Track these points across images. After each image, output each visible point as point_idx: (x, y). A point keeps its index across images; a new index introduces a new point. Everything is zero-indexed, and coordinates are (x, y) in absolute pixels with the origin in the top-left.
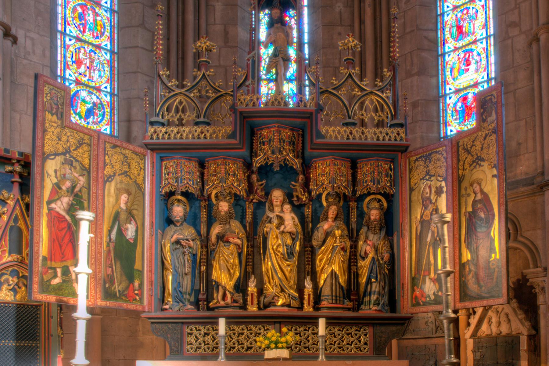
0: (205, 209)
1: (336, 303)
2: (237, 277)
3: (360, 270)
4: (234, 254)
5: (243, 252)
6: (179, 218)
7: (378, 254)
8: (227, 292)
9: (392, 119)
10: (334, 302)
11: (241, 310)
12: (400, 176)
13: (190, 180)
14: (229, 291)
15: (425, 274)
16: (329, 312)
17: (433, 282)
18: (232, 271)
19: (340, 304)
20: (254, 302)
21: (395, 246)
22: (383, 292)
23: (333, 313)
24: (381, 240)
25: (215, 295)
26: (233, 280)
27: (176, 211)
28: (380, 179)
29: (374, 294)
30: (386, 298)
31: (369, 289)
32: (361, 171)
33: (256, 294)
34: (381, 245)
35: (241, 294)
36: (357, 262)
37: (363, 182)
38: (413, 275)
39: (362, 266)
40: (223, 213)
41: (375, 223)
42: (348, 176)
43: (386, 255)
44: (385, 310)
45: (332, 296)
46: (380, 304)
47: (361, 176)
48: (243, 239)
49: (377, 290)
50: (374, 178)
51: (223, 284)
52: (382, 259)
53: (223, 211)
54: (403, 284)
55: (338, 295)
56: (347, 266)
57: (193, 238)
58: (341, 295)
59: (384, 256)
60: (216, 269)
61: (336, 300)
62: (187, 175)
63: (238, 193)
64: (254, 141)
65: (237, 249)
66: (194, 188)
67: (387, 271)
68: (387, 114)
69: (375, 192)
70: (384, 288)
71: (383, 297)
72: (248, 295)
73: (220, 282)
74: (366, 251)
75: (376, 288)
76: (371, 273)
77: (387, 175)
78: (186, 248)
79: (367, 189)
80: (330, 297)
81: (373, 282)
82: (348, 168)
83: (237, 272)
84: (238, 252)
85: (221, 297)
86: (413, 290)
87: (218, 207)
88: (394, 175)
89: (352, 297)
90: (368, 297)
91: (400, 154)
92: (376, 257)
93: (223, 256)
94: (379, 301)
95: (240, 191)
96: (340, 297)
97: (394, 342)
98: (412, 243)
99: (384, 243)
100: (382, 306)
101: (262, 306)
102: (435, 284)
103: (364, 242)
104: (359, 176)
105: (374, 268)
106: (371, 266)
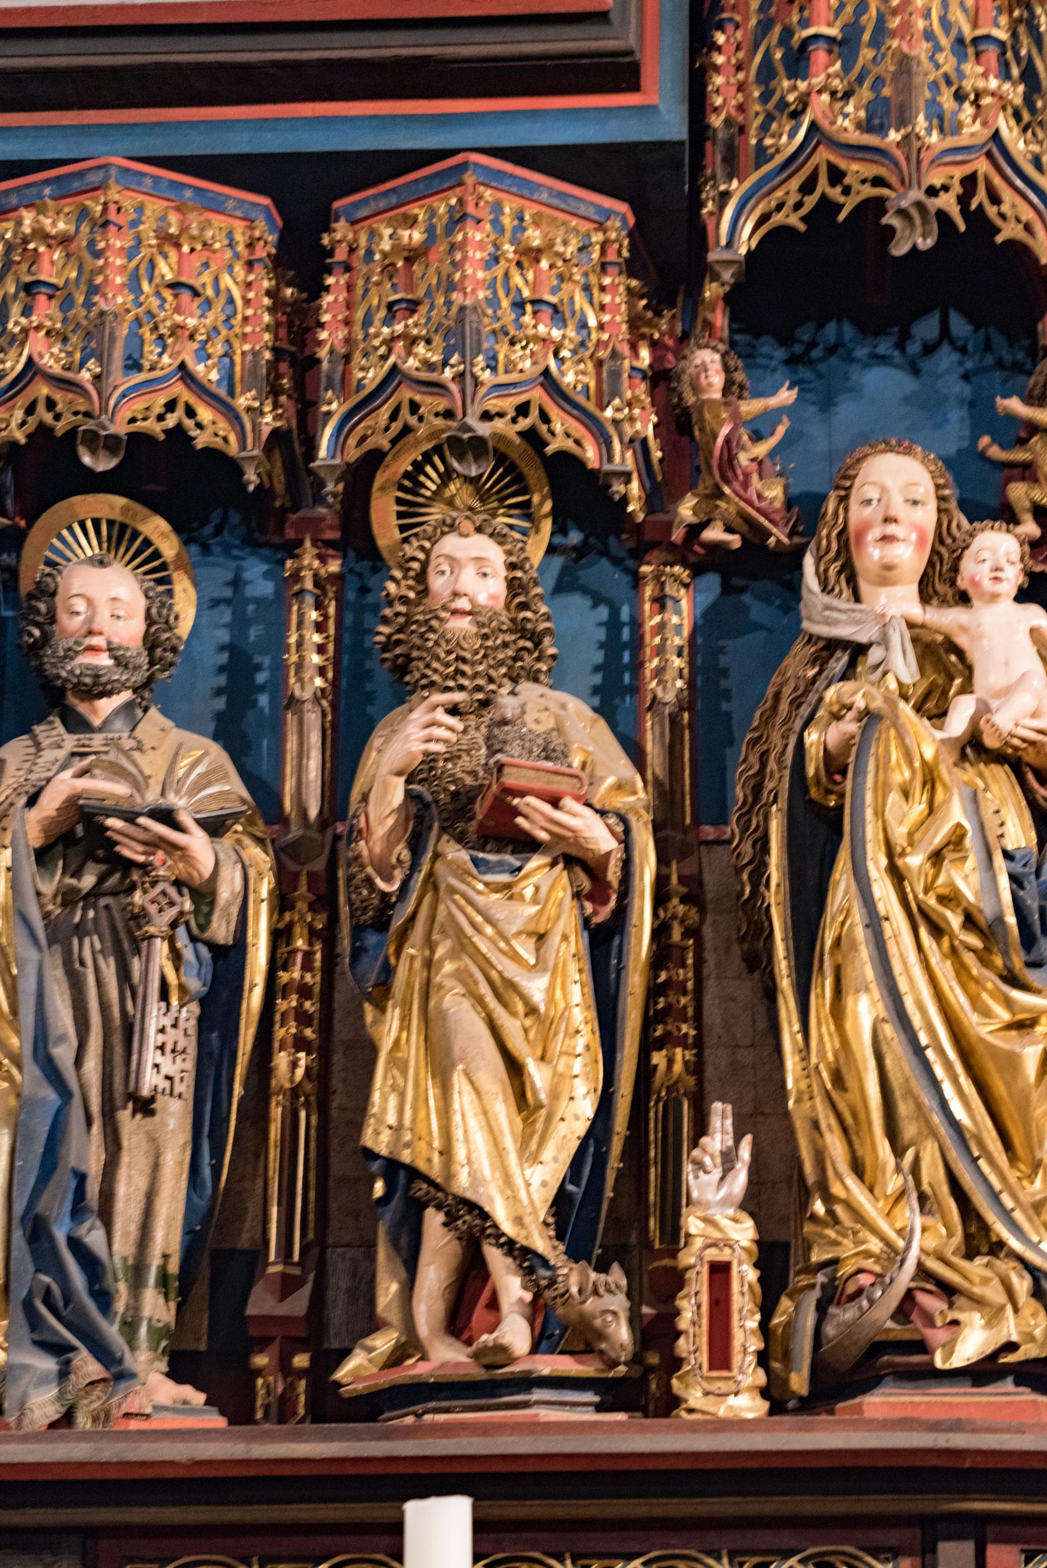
0: (319, 606)
2: (581, 1128)
4: (555, 938)
5: (635, 920)
6: (104, 660)
8: (495, 1257)
11: (621, 1416)
13: (203, 355)
14: (510, 1247)
18: (538, 1075)
20: (738, 1338)
25: (388, 1290)
26: (547, 1154)
27: (80, 605)
33: (752, 1275)
35: (617, 1276)
40: (464, 624)
48: (632, 819)
51: (462, 1183)
53: (463, 604)
57: (212, 810)
60: (398, 1063)
62: (177, 310)
63: (591, 454)
64: (720, 59)
65: (577, 895)
66: (233, 416)
72: (677, 1280)
73: (435, 1171)
78: (154, 884)
83: (581, 1087)
84: (586, 921)
85: (439, 1308)
87: (421, 577)
93: (464, 946)
95: (605, 443)
101: (799, 1382)
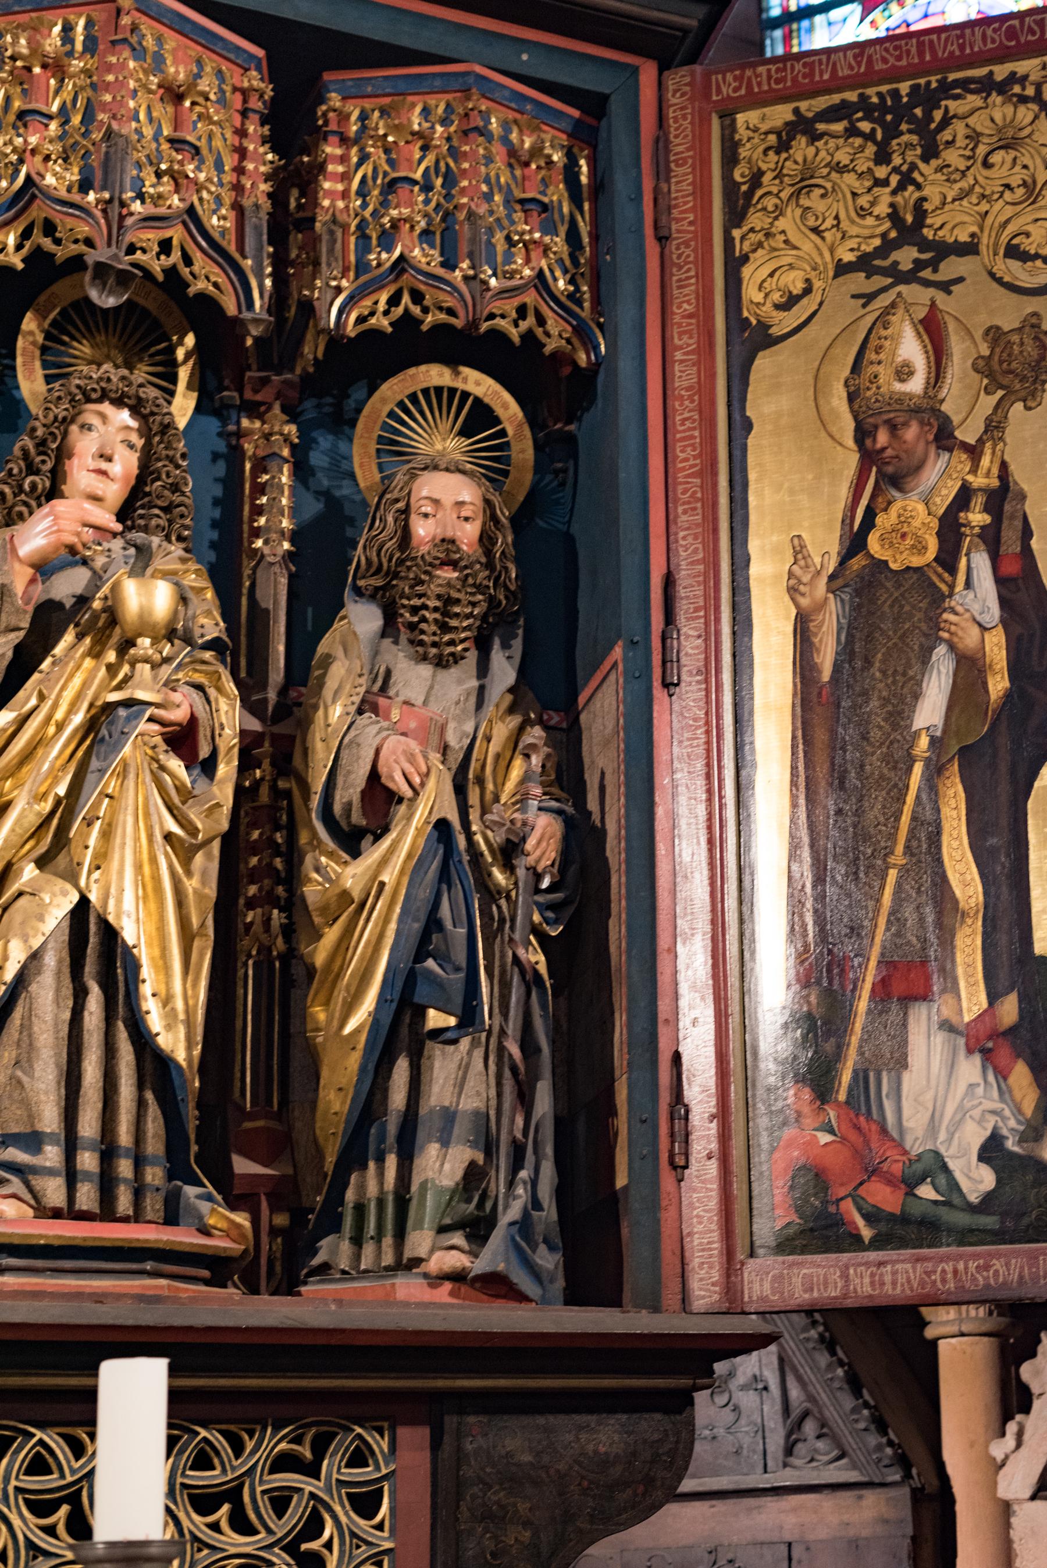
1: (107, 1212)
3: (317, 936)
10: (87, 1196)
16: (36, 1295)
17: (987, 1054)
19: (137, 1217)
22: (520, 1121)
23: (78, 1296)
24: (490, 709)
29: (445, 1143)
31: (398, 1098)
32: (343, 159)
34: (494, 748)
36: (293, 856)
37: (363, 236)
39: (345, 896)
41: (449, 574)
42: (240, 170)
45: (71, 1145)
46: (491, 1222)
47: (345, 195)
50: (447, 216)
54: (677, 1058)
55: (124, 1136)
56: (211, 891)
58: (155, 1145)
61: (107, 1183)
74: (374, 775)
75: (460, 1085)
76: (420, 955)
79: (394, 301)
80: (52, 1155)
81: (437, 1034)
82: (244, 113)
88: (595, 237)
89: (242, 1166)
90: (391, 1162)
91: (648, 72)
96: (139, 1162)
102: (1002, 1074)
103: (360, 712)
104: (329, 193)
105: (445, 911)
106: (425, 893)
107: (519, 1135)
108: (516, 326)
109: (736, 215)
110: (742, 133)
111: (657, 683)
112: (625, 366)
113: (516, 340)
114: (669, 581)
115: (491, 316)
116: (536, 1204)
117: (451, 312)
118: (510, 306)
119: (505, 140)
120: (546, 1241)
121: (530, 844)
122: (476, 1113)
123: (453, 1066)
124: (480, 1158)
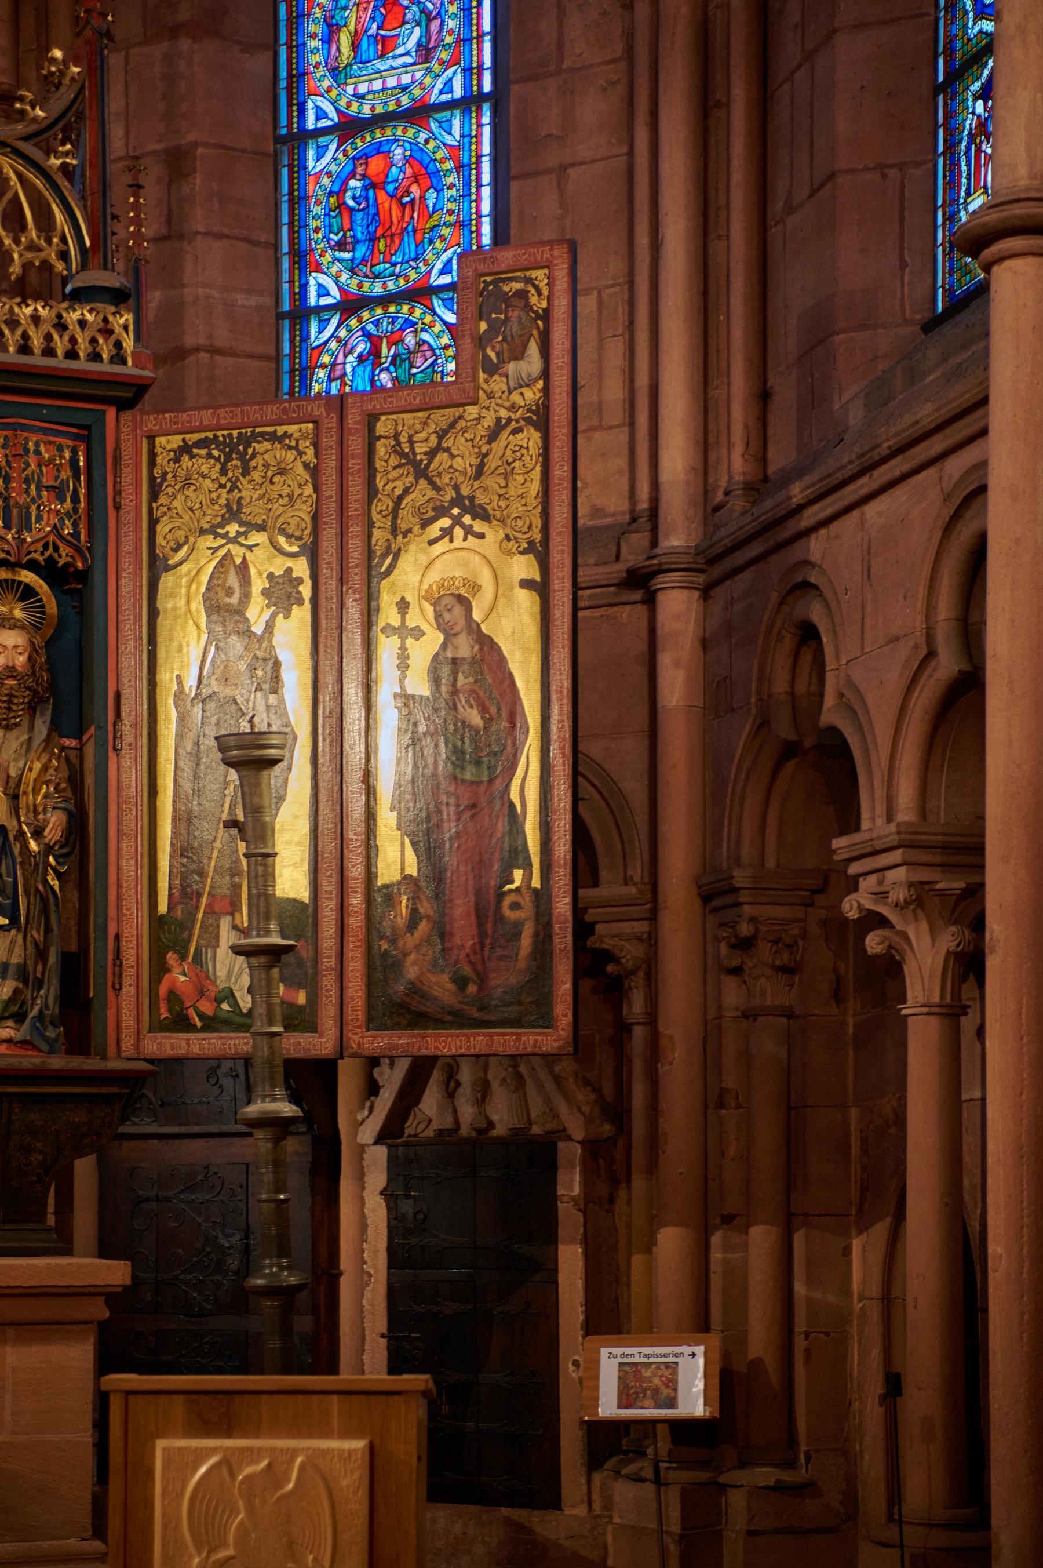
7: (22, 812)
9: (84, 266)
12: (110, 504)
15: (217, 907)
21: (89, 781)
22: (40, 967)
28: (33, 508)
30: (50, 993)
38: (163, 908)
43: (53, 820)
44: (46, 1040)
49: (15, 960)
52: (38, 834)
54: (117, 937)
59: (46, 822)
67: (55, 883)
68: (64, 240)
69: (12, 559)
70: (41, 954)
71: (40, 988)
77: (58, 492)
86: (159, 968)
91: (111, 413)
92: (15, 823)
94: (23, 1003)
97: (85, 1169)
98: (160, 782)
99: (45, 768)
100: (33, 1026)
107: (39, 976)
108: (42, 554)
109: (154, 496)
110: (158, 450)
111: (110, 749)
112: (97, 577)
113: (43, 563)
114: (118, 696)
115: (29, 553)
116: (47, 1007)
117: (8, 553)
118: (40, 546)
119: (37, 452)
120: (52, 1023)
121: (46, 833)
122: (19, 964)
123: (8, 942)
124: (21, 985)
